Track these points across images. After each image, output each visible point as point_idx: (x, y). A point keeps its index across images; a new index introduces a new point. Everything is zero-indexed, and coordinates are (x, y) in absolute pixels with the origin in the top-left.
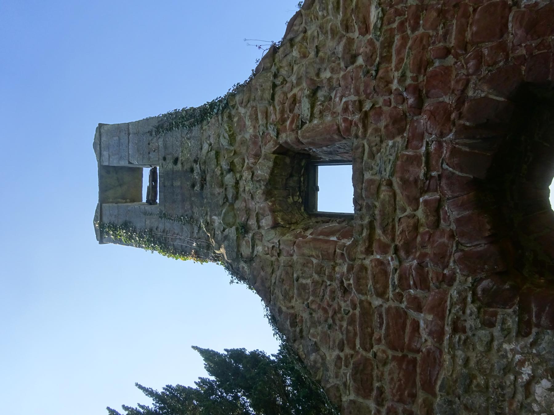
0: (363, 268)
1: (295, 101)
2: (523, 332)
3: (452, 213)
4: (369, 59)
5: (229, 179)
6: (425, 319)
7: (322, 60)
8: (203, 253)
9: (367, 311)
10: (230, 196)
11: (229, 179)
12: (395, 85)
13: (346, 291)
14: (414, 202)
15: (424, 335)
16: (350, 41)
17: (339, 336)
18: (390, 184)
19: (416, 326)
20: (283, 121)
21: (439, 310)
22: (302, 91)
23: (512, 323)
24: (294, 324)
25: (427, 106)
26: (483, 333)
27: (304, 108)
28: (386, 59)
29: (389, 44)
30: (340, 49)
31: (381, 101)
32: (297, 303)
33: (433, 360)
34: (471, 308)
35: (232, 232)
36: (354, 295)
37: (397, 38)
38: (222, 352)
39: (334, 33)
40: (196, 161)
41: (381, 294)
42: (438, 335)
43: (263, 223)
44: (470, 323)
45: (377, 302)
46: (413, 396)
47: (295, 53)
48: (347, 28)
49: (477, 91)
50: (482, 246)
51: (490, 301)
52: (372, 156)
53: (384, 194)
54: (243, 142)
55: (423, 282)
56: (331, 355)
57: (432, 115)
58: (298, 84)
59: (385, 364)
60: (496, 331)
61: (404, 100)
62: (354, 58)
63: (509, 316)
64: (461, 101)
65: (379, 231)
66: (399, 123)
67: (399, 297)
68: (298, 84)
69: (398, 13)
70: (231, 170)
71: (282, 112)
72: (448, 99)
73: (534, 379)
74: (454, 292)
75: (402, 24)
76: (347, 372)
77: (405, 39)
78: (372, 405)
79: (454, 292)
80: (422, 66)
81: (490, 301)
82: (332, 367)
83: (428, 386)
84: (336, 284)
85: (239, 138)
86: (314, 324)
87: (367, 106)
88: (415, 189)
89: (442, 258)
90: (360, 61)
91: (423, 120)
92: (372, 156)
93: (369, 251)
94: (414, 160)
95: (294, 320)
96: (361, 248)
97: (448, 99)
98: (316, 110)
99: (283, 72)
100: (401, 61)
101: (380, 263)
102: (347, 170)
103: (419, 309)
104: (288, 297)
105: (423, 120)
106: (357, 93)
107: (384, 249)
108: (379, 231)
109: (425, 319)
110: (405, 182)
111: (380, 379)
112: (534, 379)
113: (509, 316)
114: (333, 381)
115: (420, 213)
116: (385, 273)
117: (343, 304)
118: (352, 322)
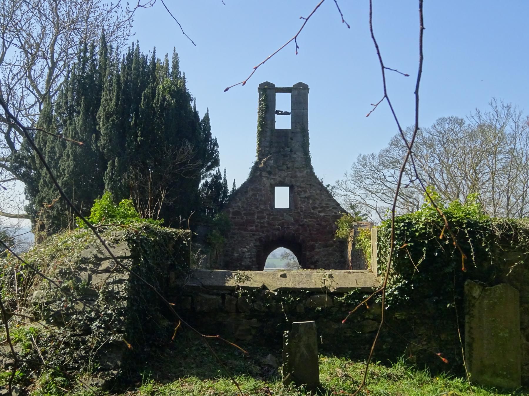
0: (263, 213)
1: (305, 192)
2: (256, 246)
3: (277, 233)
4: (312, 214)
5: (285, 167)
6: (254, 228)
7: (314, 200)
8: (261, 154)
9: (253, 214)
10: (280, 168)
11: (285, 167)
12: (305, 220)
13: (257, 208)
14: (279, 225)
15: (251, 228)
16: (317, 208)
17: (245, 206)
18: (283, 219)
19: (252, 226)
20: (301, 188)
21: (257, 231)
22: (307, 195)
23: (256, 244)
24: (245, 192)
25: (300, 227)
26: (253, 239)
27: (303, 195)
28: (311, 218)
29: (314, 218)
30: (316, 205)
31: (302, 216)
32: (251, 193)
33: (246, 230)
34: (258, 237)
35: (269, 169)
36: (257, 210)
37: (315, 220)
38: (213, 137)
39: (321, 203)
40: (291, 151)
41: (258, 218)
42: (251, 231)
43: (272, 181)
44: (255, 237)
45: (256, 217)
46: (236, 225)
47: (318, 192)
48: (322, 207)
49: (301, 237)
50: (271, 238)
51: (260, 240)
52: (290, 215)
53: (281, 218)
54: (296, 172)
55: (262, 227)
56: (240, 204)
57: (298, 228)
58: (311, 193)
59: (242, 219)
60: (254, 242)
61: (301, 222)
62: (313, 209)
63: (258, 244)
64: (300, 234)
65: (272, 217)
66: (296, 221)
67: (258, 222)
68: (311, 193)
69: (321, 220)
70: (288, 168)
71: (303, 187)
72: (301, 232)
73: (247, 248)
74: (261, 234)
75: (318, 221)
76: (236, 209)
77: (315, 222)
78: (231, 216)
79: (261, 234)
80: (308, 226)
81: (260, 240)
82: (236, 205)
83: (239, 229)
84: (258, 205)
85: (297, 170)
86: (247, 199)
87: (301, 213)
88: (282, 225)
89: (267, 231)
90: (312, 211)
91: (297, 226)
92: (290, 215)
93: (267, 214)
94: (288, 225)
95: (246, 192)
96: (268, 212)
97: (301, 232)
98: (302, 199)
99: (314, 188)
100: (310, 221)
101: (265, 218)
102: (287, 189)
103: (256, 227)
104: (252, 189)
105: (297, 226)
106: (305, 210)
107: (268, 218)
108: (272, 217)
109: (254, 228)
110: (283, 223)
111: (238, 218)
112: (247, 248)
113: (258, 244)
114: (233, 205)
115: (277, 226)
116: (263, 218)
117: (253, 208)
118: (250, 210)
